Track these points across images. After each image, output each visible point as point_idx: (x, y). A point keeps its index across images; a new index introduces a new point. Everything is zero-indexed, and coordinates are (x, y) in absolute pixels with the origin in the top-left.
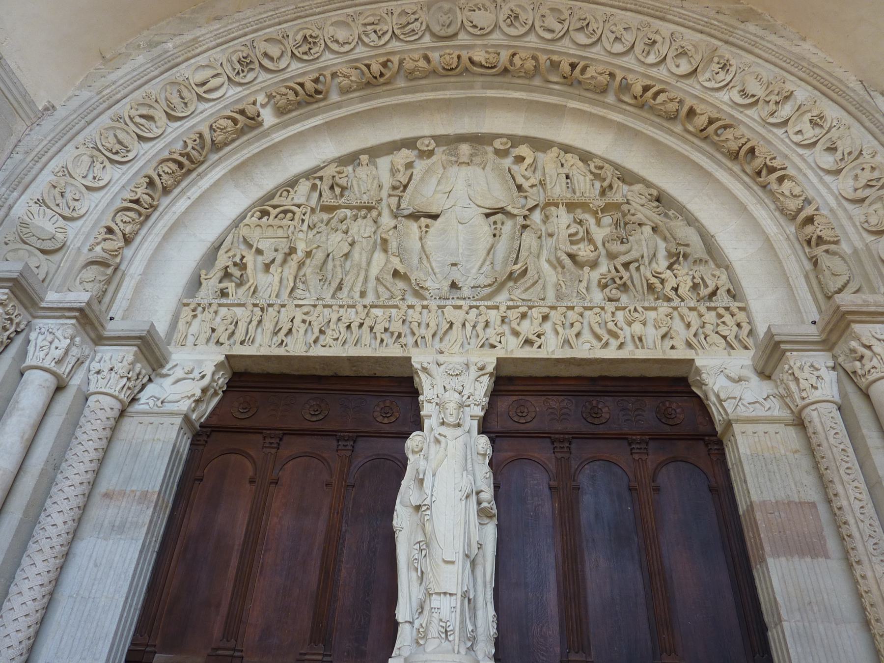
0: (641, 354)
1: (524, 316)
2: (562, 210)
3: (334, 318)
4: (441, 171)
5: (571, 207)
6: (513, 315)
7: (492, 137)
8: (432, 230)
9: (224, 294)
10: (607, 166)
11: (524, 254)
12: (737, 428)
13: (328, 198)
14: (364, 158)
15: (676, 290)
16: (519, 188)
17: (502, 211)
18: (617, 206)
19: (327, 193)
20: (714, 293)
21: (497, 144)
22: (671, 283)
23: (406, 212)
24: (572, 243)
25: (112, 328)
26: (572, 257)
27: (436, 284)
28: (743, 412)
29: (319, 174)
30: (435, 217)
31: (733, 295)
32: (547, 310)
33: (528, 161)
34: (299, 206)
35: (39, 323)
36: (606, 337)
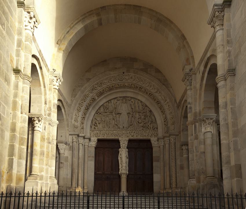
0: (145, 138)
1: (132, 132)
2: (137, 113)
3: (109, 132)
4: (121, 104)
5: (138, 112)
6: (131, 132)
7: (129, 97)
8: (120, 117)
9: (95, 128)
10: (144, 104)
11: (132, 121)
12: (154, 148)
13: (106, 111)
14: (110, 101)
15: (150, 128)
16: (132, 108)
17: (129, 113)
18: (145, 112)
19: (105, 110)
20: (155, 128)
21: (129, 99)
22: (150, 127)
23: (117, 113)
24: (139, 119)
25: (86, 137)
26: (138, 122)
27: (121, 127)
28: (155, 146)
29: (103, 105)
30: (121, 114)
31: (157, 128)
32: (134, 131)
33: (133, 103)
34: (102, 112)
35: (79, 138)
36: (141, 135)
